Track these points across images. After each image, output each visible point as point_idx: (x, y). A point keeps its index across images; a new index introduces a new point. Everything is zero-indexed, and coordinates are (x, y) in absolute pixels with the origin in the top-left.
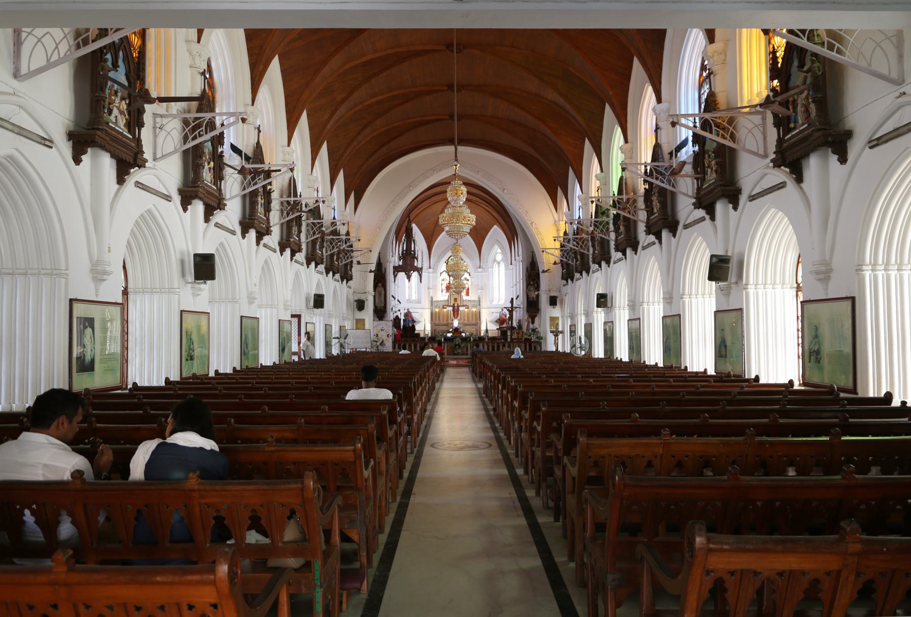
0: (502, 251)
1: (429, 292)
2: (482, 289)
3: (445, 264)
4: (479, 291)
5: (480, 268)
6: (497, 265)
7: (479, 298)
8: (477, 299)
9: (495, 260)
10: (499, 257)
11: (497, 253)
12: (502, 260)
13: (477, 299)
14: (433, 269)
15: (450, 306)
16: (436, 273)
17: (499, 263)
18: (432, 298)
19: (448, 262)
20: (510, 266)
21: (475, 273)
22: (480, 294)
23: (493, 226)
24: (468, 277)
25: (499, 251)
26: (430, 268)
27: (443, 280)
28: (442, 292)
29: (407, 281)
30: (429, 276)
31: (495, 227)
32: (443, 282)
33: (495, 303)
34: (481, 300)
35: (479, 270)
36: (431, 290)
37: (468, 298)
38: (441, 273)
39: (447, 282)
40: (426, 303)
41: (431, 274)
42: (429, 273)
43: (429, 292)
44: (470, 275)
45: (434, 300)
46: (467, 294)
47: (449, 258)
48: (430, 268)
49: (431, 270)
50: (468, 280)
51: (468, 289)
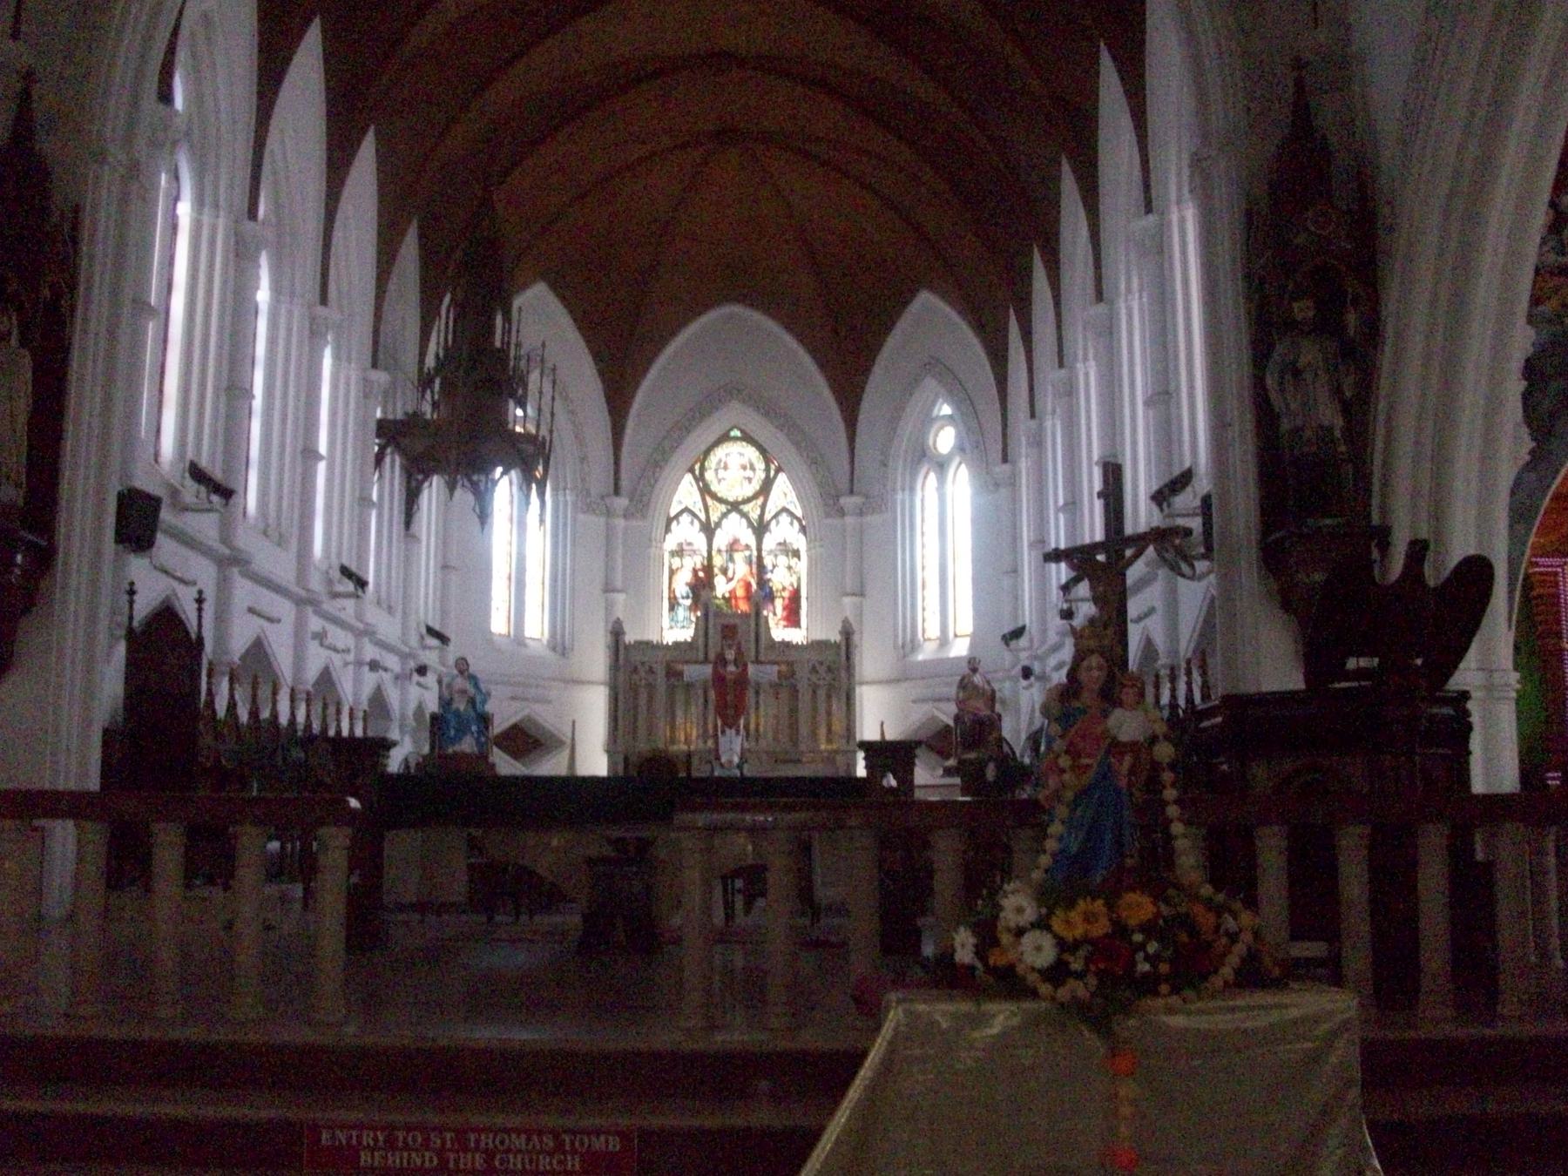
0: (957, 405)
1: (609, 607)
2: (862, 595)
3: (688, 477)
4: (847, 600)
5: (852, 492)
6: (932, 476)
7: (847, 633)
8: (835, 636)
9: (922, 455)
10: (945, 439)
11: (927, 420)
12: (960, 448)
13: (835, 636)
14: (631, 500)
15: (706, 660)
16: (644, 517)
17: (941, 465)
18: (617, 633)
19: (703, 469)
20: (1002, 470)
21: (828, 515)
22: (848, 614)
23: (913, 293)
24: (800, 542)
25: (946, 410)
26: (617, 491)
27: (679, 552)
28: (672, 608)
29: (478, 527)
30: (609, 533)
31: (925, 300)
32: (676, 562)
33: (926, 653)
34: (856, 638)
35: (848, 502)
36: (620, 597)
37: (797, 636)
38: (669, 521)
39: (698, 561)
40: (595, 661)
41: (620, 523)
42: (609, 513)
43: (609, 607)
44: (803, 529)
45: (630, 638)
46: (792, 618)
47: (707, 453)
48: (617, 491)
49: (622, 502)
50: (796, 554)
51: (795, 597)
